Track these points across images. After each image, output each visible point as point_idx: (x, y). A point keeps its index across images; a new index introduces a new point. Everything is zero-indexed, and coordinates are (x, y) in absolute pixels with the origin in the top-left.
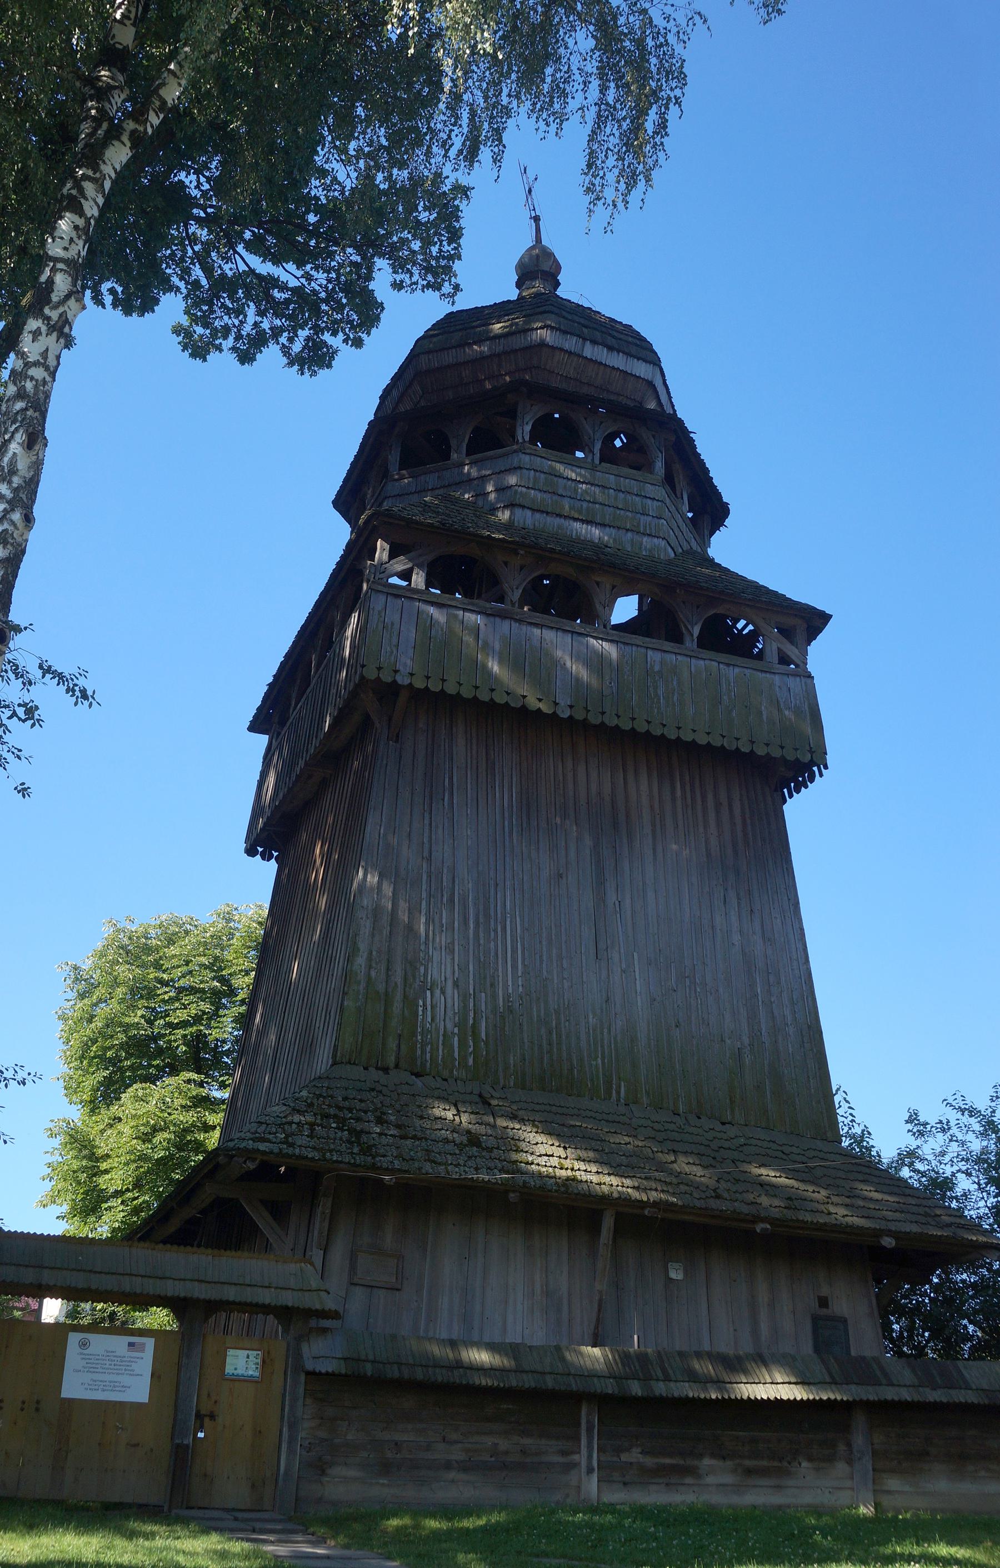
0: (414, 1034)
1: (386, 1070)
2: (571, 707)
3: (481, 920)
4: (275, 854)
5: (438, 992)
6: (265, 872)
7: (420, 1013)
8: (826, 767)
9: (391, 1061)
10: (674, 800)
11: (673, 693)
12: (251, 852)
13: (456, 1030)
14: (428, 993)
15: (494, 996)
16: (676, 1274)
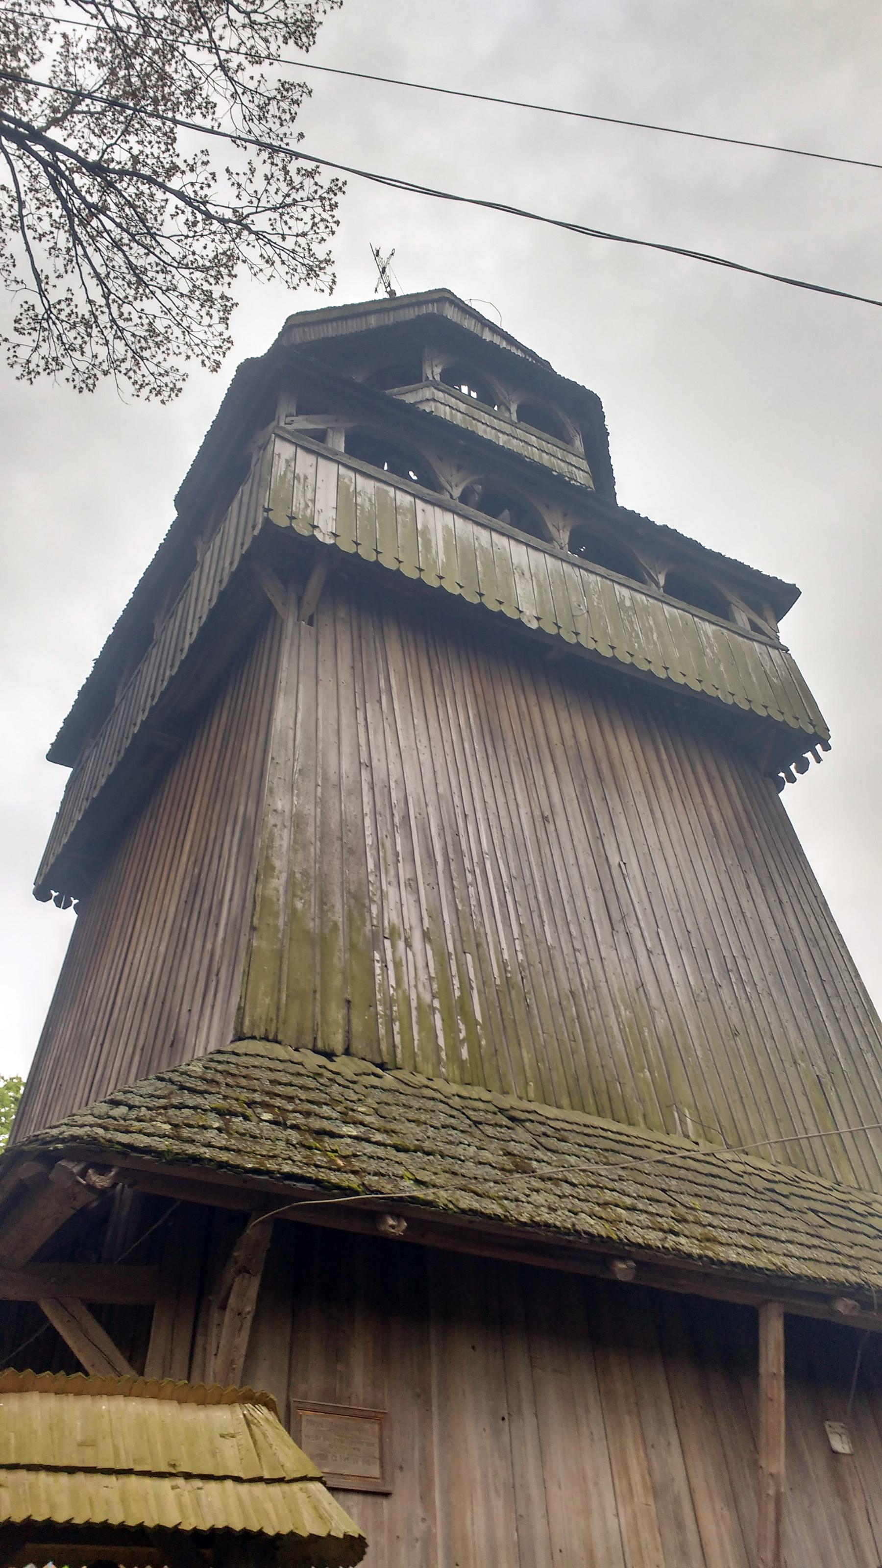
0: (372, 1004)
1: (330, 1055)
2: (538, 619)
3: (451, 856)
4: (75, 902)
5: (401, 944)
6: (60, 922)
7: (378, 971)
8: (827, 748)
9: (337, 1042)
10: (660, 761)
11: (652, 632)
12: (41, 894)
13: (436, 1004)
14: (387, 943)
15: (481, 962)
16: (840, 1445)
